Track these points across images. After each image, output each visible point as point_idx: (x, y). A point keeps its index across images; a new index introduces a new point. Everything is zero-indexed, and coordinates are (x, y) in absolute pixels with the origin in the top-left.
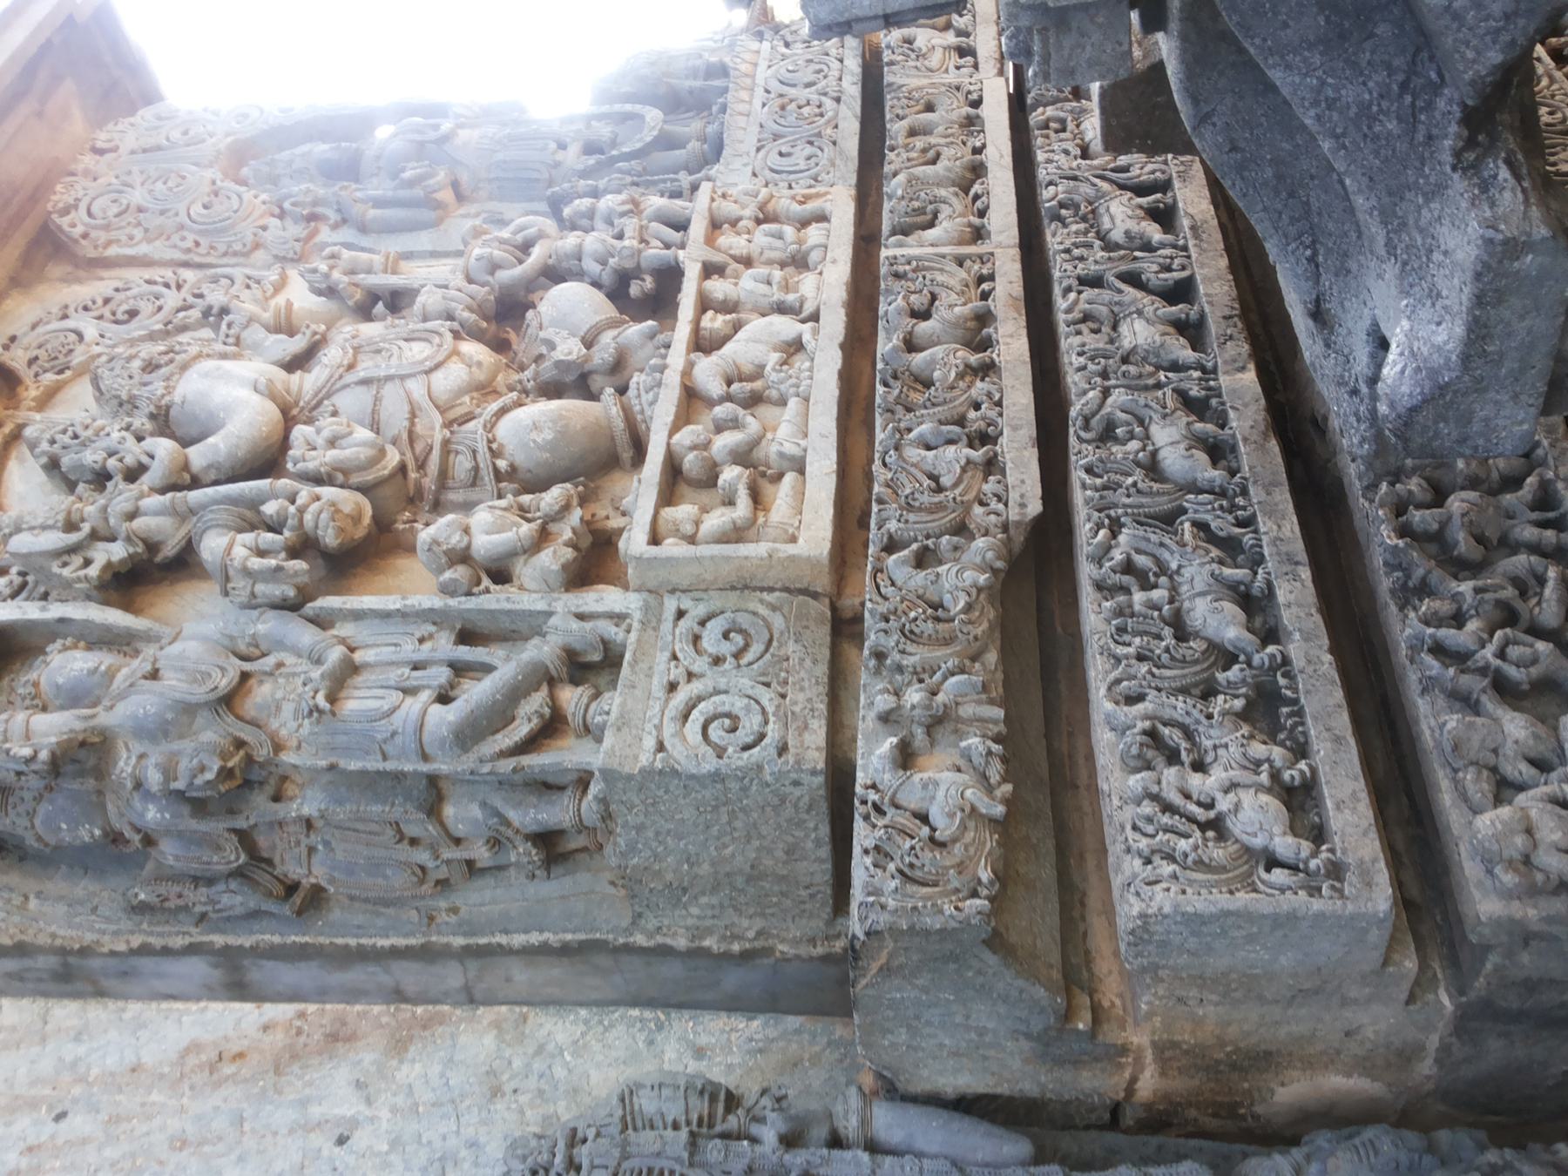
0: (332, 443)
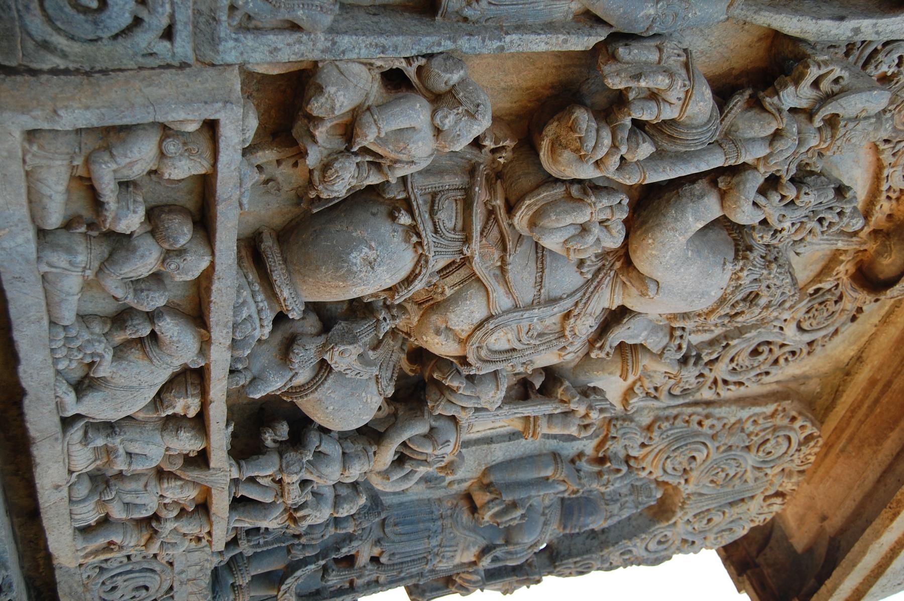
0: (584, 229)
